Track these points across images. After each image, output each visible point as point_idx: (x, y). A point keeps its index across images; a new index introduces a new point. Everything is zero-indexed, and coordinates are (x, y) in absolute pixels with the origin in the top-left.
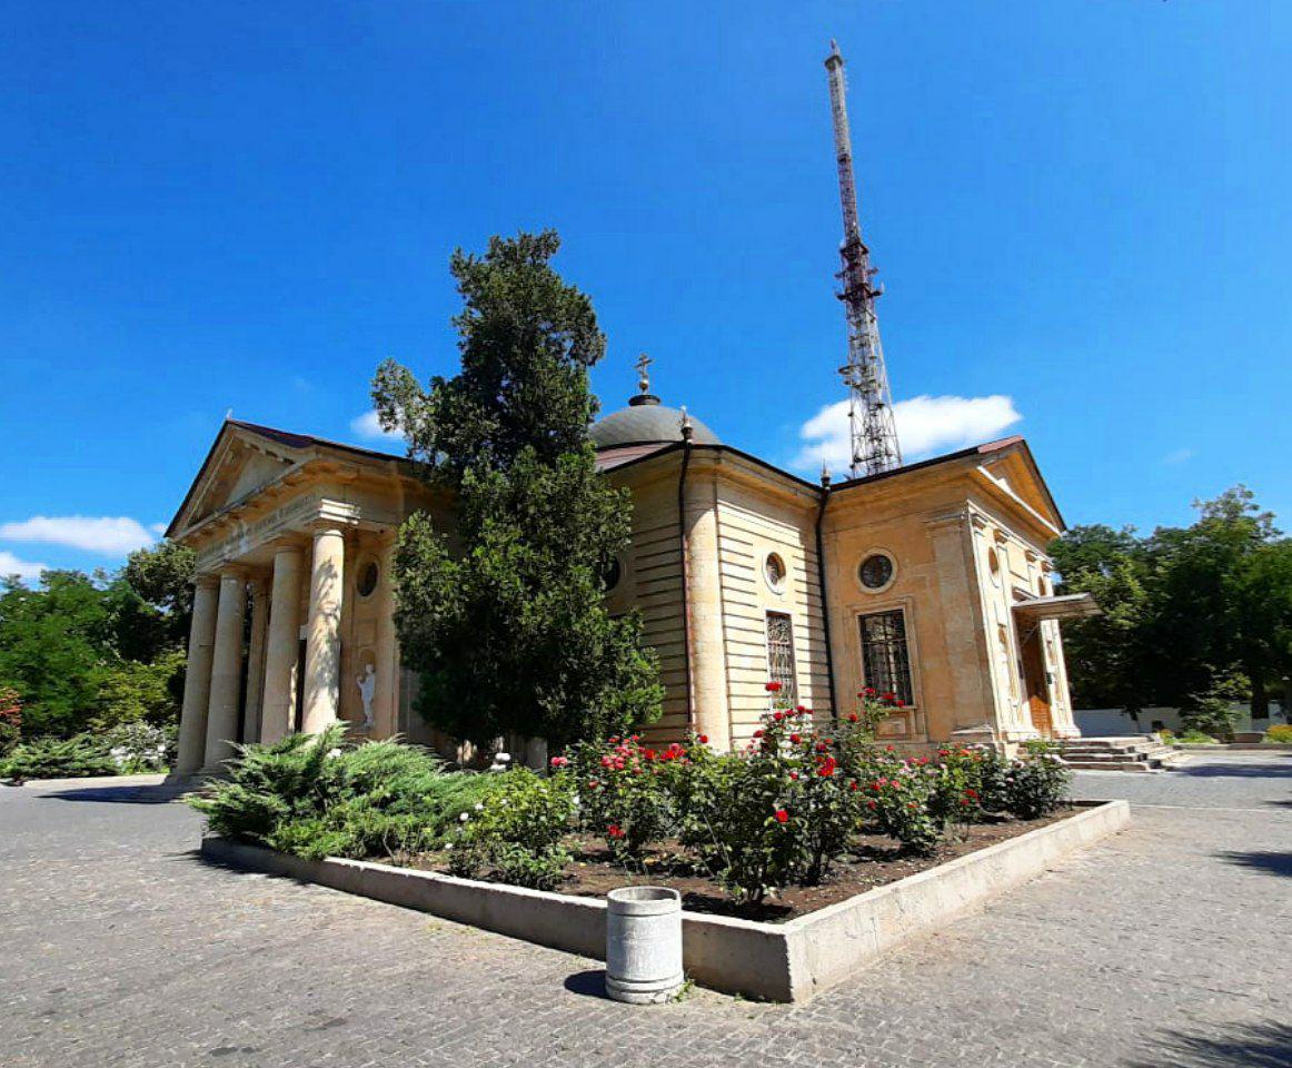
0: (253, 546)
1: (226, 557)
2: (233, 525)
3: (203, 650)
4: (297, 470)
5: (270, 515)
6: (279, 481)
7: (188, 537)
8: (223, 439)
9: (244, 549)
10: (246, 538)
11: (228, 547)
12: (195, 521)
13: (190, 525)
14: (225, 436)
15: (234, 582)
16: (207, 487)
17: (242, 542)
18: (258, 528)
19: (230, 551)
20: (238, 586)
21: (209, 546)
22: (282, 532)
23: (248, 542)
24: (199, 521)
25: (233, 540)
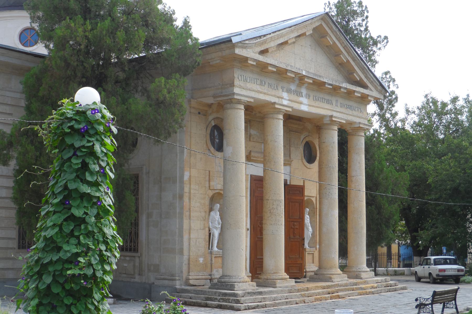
11: (285, 95)
22: (346, 120)
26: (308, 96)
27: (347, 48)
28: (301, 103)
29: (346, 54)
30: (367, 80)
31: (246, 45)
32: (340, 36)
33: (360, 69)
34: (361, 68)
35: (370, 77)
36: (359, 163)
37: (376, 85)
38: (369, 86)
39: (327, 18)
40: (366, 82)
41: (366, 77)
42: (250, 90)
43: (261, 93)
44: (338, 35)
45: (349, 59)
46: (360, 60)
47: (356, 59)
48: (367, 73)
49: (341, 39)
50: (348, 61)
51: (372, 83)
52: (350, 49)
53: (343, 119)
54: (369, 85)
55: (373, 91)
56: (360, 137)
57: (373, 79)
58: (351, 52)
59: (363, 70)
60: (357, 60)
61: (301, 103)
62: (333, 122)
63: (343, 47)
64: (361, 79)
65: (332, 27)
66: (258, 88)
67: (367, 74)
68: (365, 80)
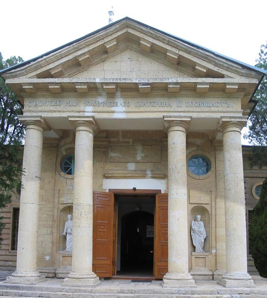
26: (126, 104)
27: (172, 43)
28: (113, 112)
29: (174, 50)
30: (218, 68)
32: (156, 34)
33: (203, 60)
34: (203, 57)
35: (221, 63)
36: (229, 160)
37: (236, 69)
39: (131, 23)
40: (217, 70)
41: (216, 65)
42: (41, 112)
43: (55, 112)
44: (153, 34)
45: (181, 53)
46: (197, 49)
47: (190, 50)
48: (214, 60)
49: (159, 37)
50: (180, 56)
51: (227, 69)
52: (176, 43)
53: (184, 116)
54: (224, 72)
55: (234, 78)
56: (229, 132)
57: (227, 64)
58: (179, 45)
59: (207, 58)
60: (192, 51)
61: (113, 112)
62: (171, 123)
63: (168, 44)
64: (209, 70)
65: (142, 30)
66: (53, 108)
67: (215, 62)
68: (216, 69)
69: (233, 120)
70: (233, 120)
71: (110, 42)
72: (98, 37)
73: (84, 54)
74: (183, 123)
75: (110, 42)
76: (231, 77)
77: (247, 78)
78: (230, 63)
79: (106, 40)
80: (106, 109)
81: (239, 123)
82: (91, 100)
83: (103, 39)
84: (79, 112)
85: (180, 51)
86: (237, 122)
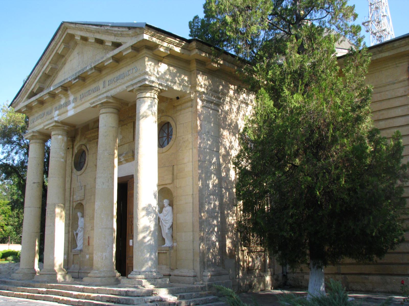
0: (79, 110)
1: (56, 119)
2: (62, 96)
3: (35, 185)
4: (126, 49)
5: (93, 86)
6: (108, 59)
7: (26, 106)
8: (58, 35)
9: (71, 113)
10: (72, 105)
11: (57, 112)
12: (33, 94)
13: (29, 97)
14: (60, 32)
15: (60, 137)
16: (43, 69)
17: (70, 107)
18: (83, 97)
19: (58, 115)
20: (63, 140)
21: (41, 113)
22: (107, 97)
23: (74, 108)
24: (35, 94)
25: (60, 107)
31: (16, 103)
35: (116, 32)
38: (120, 41)
51: (122, 35)
69: (135, 87)
70: (135, 87)
71: (60, 48)
72: (52, 49)
73: (48, 67)
74: (104, 104)
75: (60, 48)
76: (125, 43)
77: (136, 37)
78: (121, 29)
79: (57, 48)
80: (63, 110)
81: (142, 88)
82: (57, 105)
83: (55, 48)
84: (51, 119)
85: (95, 34)
86: (139, 88)
